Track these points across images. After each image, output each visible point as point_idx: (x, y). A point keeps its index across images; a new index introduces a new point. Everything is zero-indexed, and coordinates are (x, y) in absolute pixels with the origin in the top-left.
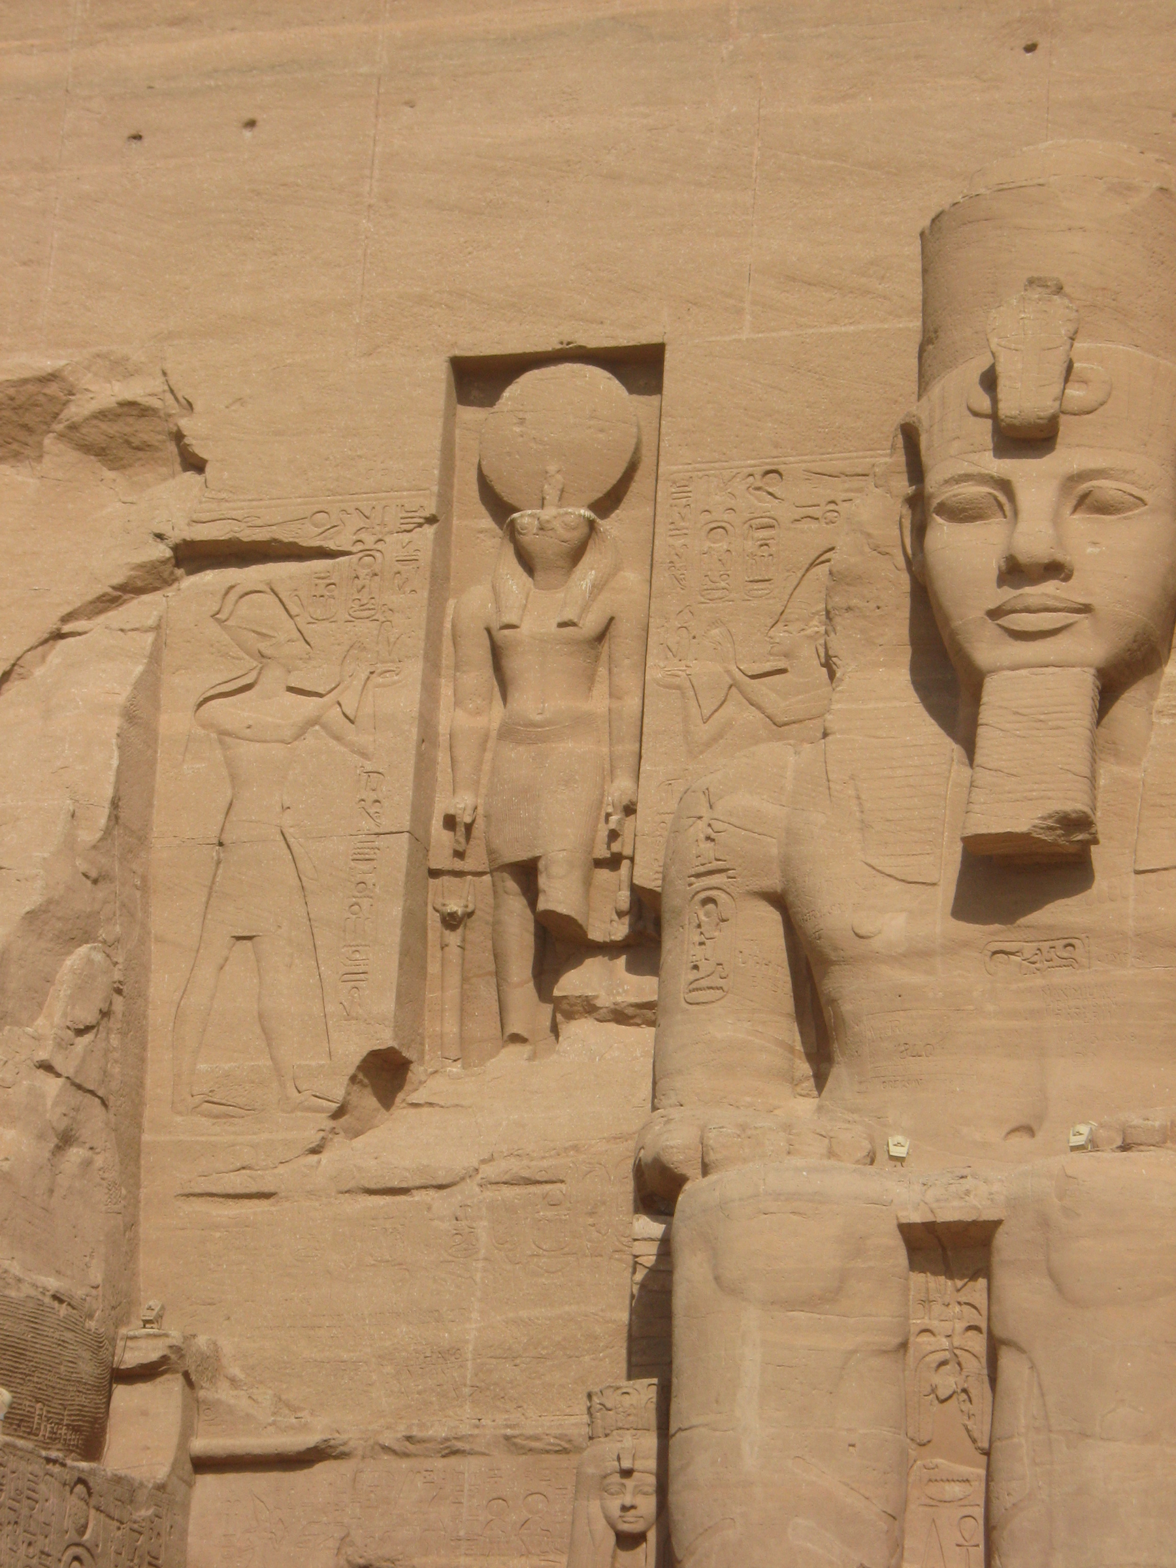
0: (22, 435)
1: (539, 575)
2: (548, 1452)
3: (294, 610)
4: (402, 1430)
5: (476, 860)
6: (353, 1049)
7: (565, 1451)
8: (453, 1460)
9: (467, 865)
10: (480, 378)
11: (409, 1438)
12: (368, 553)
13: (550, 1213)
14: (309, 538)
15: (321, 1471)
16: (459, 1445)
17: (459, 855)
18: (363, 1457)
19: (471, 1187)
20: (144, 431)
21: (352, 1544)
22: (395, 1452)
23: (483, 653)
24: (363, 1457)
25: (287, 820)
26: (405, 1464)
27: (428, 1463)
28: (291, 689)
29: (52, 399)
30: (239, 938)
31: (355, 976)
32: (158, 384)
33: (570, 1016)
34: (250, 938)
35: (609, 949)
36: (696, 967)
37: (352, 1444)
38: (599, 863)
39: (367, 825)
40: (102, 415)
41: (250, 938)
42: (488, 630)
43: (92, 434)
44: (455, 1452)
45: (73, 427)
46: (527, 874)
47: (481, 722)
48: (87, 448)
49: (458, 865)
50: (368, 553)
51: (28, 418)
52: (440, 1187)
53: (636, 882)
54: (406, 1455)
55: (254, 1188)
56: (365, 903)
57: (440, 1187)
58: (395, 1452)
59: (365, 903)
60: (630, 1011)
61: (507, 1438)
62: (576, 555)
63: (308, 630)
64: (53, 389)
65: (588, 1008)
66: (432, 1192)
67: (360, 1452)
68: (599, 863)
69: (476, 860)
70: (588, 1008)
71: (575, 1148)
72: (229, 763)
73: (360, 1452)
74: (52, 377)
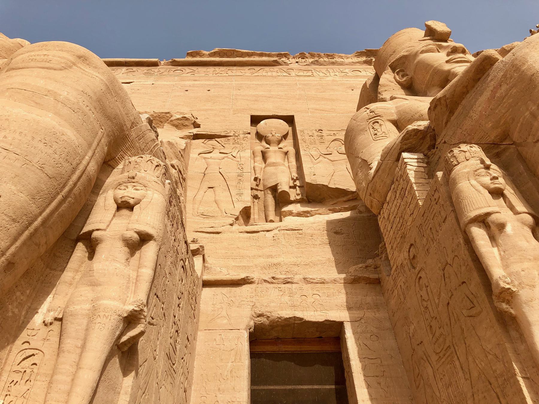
0: (160, 123)
1: (271, 145)
2: (317, 283)
3: (220, 142)
4: (270, 277)
5: (261, 187)
6: (240, 207)
7: (323, 283)
8: (287, 285)
9: (259, 188)
10: (255, 120)
11: (273, 278)
12: (237, 136)
13: (300, 236)
14: (223, 134)
15: (245, 288)
16: (289, 280)
17: (257, 185)
18: (258, 284)
19: (276, 231)
20: (186, 123)
21: (256, 307)
22: (269, 282)
23: (260, 155)
24: (258, 284)
25: (221, 170)
26: (272, 285)
27: (279, 286)
28: (220, 153)
29: (167, 117)
30: (209, 188)
31: (240, 194)
32: (191, 116)
33: (285, 216)
34: (212, 188)
35: (296, 202)
36: (376, 134)
37: (254, 279)
38: (290, 187)
39: (240, 171)
40: (178, 119)
41: (212, 188)
42: (262, 151)
43: (176, 122)
44: (288, 283)
45: (171, 121)
46: (274, 189)
47: (261, 165)
48: (174, 125)
49: (257, 188)
50: (237, 136)
51: (162, 120)
52: (268, 231)
53: (308, 179)
54: (272, 283)
55: (215, 231)
56: (241, 183)
57: (268, 231)
58: (269, 282)
59: (241, 183)
60: (302, 213)
61: (304, 279)
62: (279, 142)
63: (224, 145)
64: (168, 115)
65: (290, 213)
66: (265, 232)
67: (257, 282)
68: (290, 187)
69: (261, 187)
70: (290, 213)
71: (303, 225)
72: (206, 162)
73: (257, 282)
74: (169, 113)
